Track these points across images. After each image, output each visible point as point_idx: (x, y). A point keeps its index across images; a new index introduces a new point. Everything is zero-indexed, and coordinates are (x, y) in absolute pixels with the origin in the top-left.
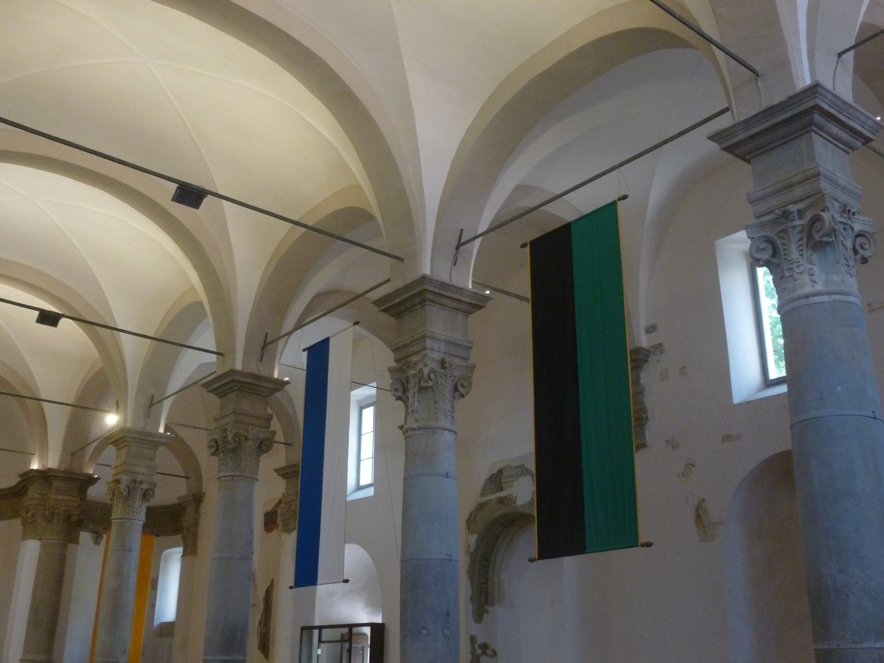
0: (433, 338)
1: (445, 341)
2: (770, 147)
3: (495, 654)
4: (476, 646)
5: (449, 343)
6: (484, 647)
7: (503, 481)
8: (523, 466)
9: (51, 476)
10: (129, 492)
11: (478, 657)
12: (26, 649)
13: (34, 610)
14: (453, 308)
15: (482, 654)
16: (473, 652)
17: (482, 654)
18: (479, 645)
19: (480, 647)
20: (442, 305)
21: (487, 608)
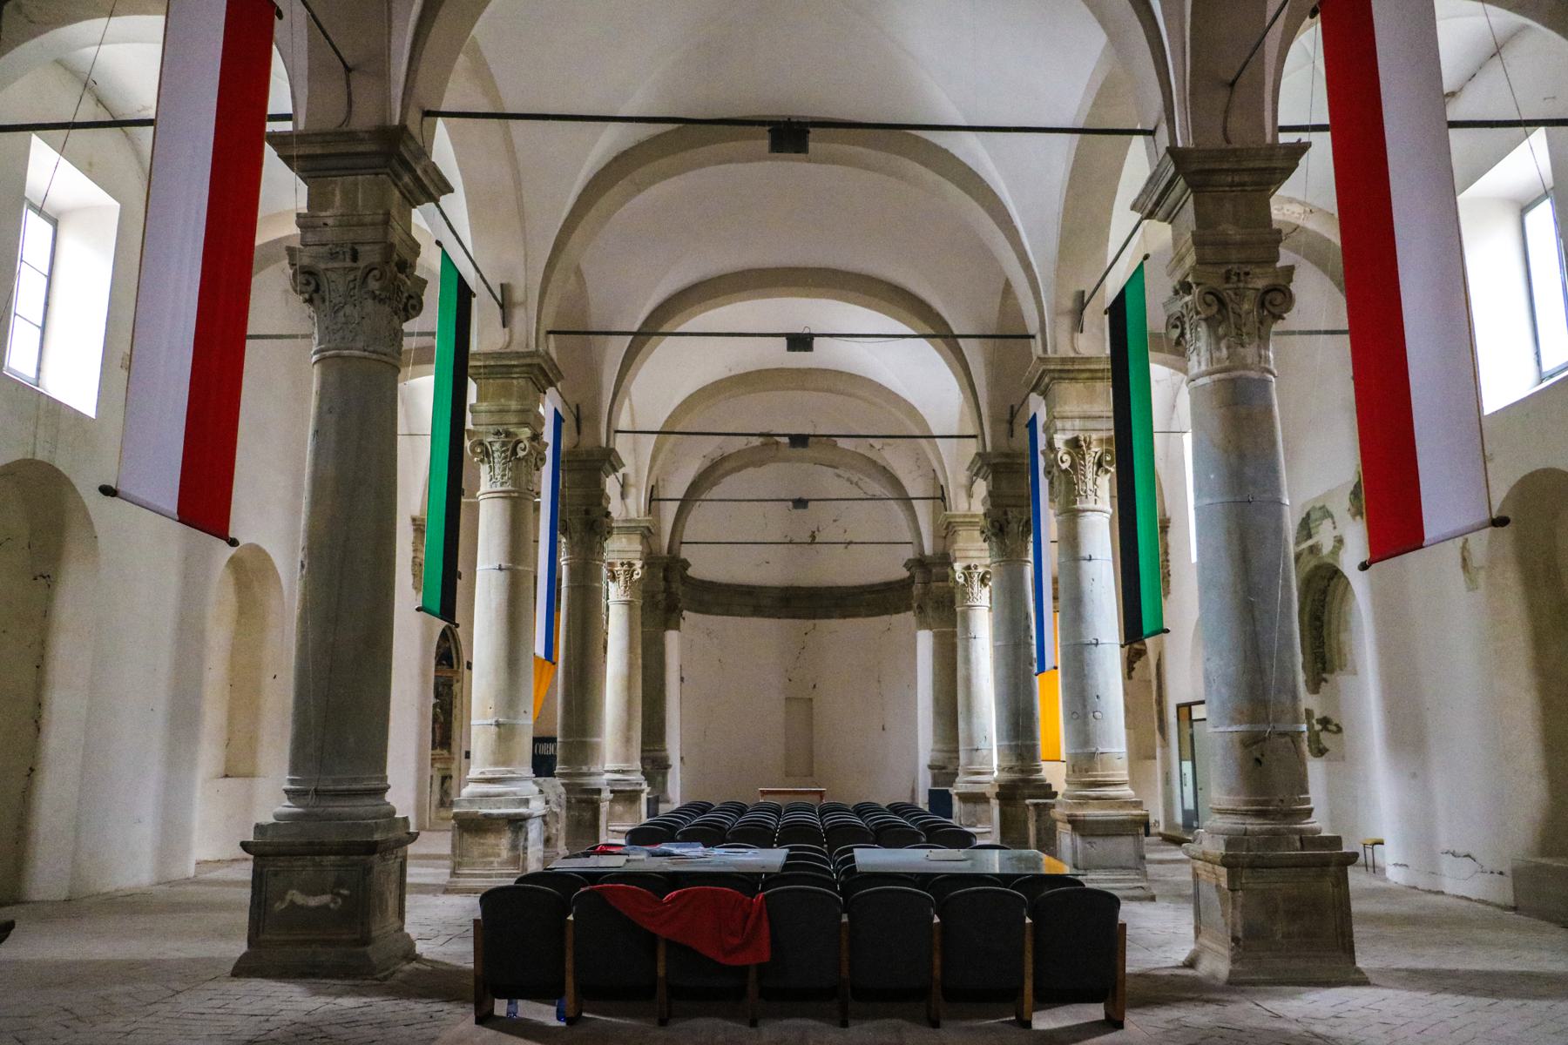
0: (1063, 418)
1: (1080, 418)
2: (1175, 212)
3: (1339, 730)
4: (1314, 721)
5: (1084, 418)
6: (1325, 722)
7: (1312, 525)
8: (1324, 507)
9: (927, 564)
10: (966, 580)
11: (1317, 734)
12: (935, 742)
13: (936, 701)
14: (1088, 379)
15: (1322, 730)
17: (1322, 730)
18: (1317, 720)
19: (1319, 721)
21: (1324, 675)
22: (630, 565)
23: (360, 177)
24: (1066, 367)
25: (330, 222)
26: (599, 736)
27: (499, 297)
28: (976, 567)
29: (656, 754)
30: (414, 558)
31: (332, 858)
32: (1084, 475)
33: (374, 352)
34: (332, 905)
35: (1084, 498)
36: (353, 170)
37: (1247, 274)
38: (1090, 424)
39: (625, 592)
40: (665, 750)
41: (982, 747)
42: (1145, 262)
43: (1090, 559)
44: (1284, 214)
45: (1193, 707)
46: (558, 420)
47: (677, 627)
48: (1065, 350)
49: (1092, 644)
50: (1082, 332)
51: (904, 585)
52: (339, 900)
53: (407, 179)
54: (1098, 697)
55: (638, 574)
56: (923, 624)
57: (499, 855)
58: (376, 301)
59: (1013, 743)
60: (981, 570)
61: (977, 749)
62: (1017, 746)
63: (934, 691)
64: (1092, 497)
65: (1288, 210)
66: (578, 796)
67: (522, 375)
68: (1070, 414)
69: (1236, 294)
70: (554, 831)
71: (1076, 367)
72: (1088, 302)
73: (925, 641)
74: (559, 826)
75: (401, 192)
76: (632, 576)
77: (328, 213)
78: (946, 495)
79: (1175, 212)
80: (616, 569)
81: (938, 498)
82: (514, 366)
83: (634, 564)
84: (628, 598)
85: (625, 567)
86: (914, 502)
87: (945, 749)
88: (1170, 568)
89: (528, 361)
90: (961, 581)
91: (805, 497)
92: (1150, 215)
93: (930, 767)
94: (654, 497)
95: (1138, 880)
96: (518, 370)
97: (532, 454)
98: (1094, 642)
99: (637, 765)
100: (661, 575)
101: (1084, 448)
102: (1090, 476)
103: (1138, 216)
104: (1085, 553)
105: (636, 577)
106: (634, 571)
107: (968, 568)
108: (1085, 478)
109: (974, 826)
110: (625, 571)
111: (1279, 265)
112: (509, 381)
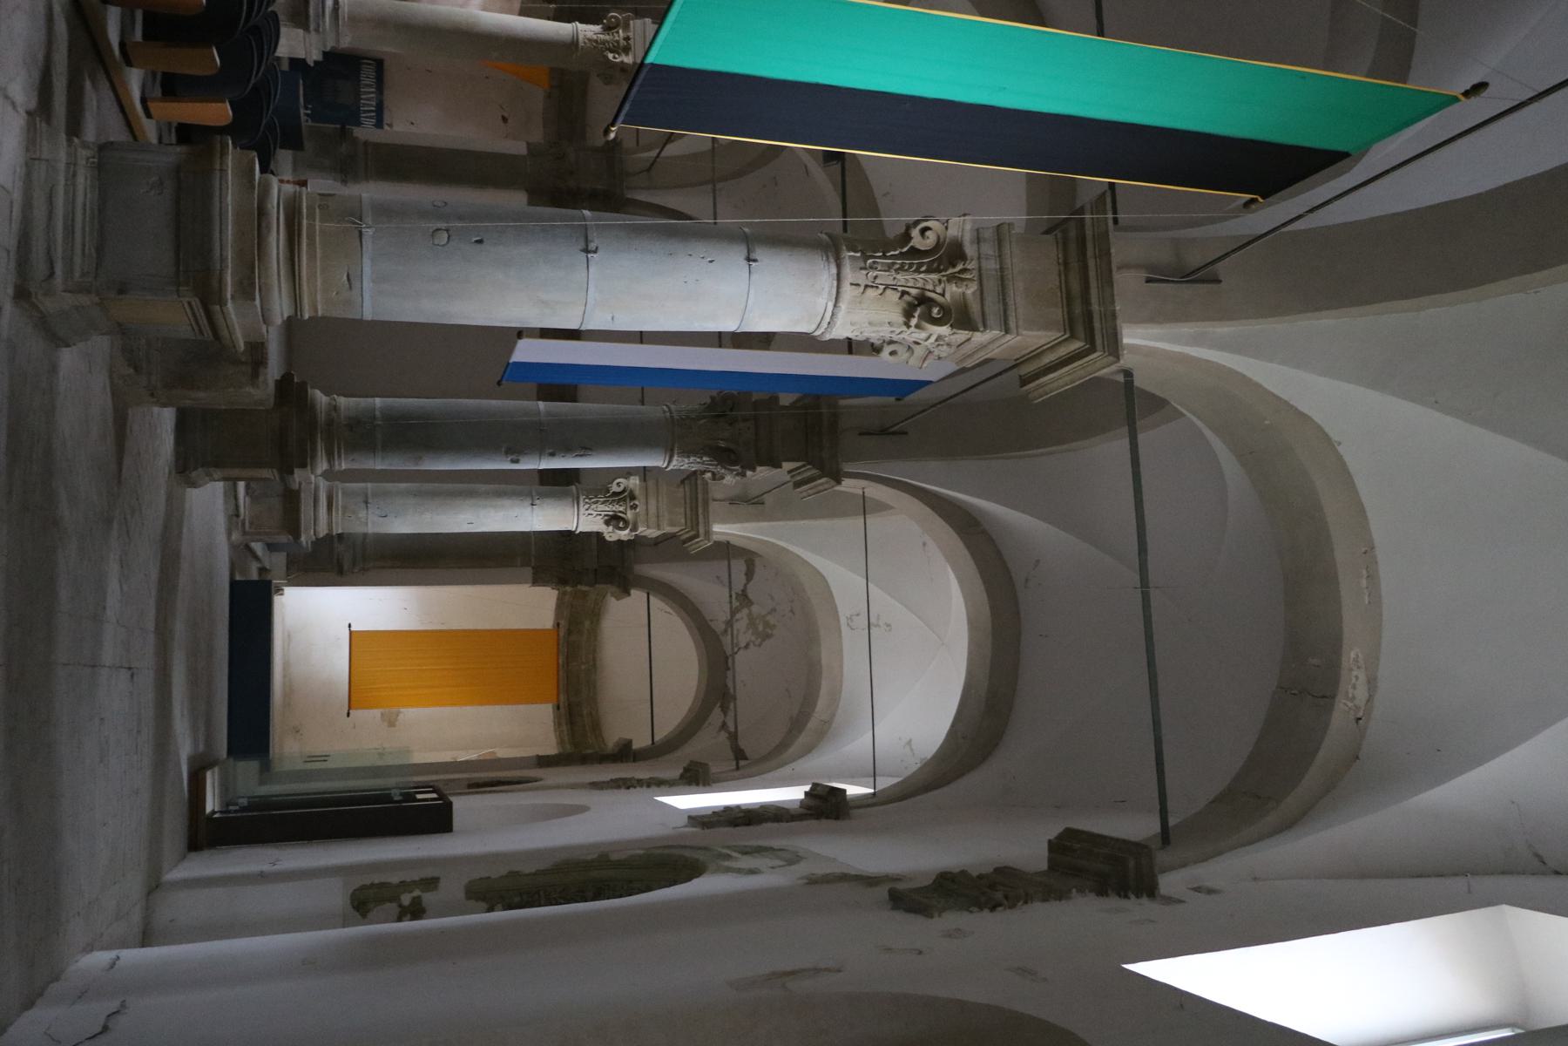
4: (416, 893)
5: (1002, 279)
10: (615, 494)
11: (395, 898)
15: (400, 906)
16: (405, 886)
17: (400, 906)
20: (1066, 264)
22: (626, 50)
24: (1090, 246)
28: (634, 507)
32: (901, 269)
35: (862, 265)
38: (991, 286)
39: (589, 40)
41: (370, 511)
43: (749, 259)
44: (1351, 670)
48: (1123, 248)
49: (587, 241)
50: (1149, 281)
54: (480, 242)
55: (614, 58)
59: (377, 413)
60: (630, 515)
61: (366, 502)
62: (374, 418)
64: (861, 277)
65: (1357, 677)
68: (1007, 251)
71: (1091, 263)
80: (621, 31)
83: (627, 54)
84: (581, 44)
85: (623, 43)
87: (367, 541)
88: (638, 789)
90: (615, 488)
95: (69, 271)
98: (592, 246)
99: (346, 42)
100: (600, 187)
101: (951, 271)
102: (902, 278)
104: (759, 253)
105: (610, 56)
106: (619, 54)
107: (633, 497)
108: (897, 271)
110: (618, 42)
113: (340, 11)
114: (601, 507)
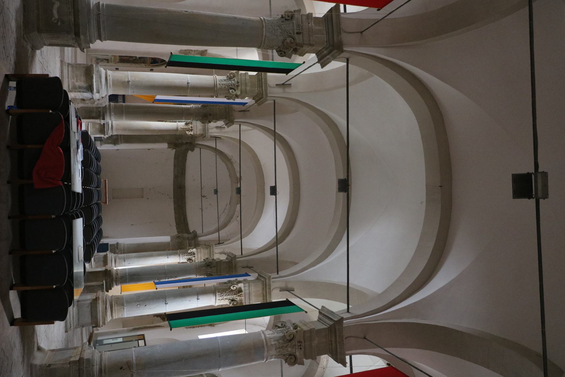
9: (195, 239)
10: (190, 253)
12: (127, 245)
22: (192, 130)
23: (325, 36)
25: (310, 25)
26: (125, 120)
27: (286, 83)
29: (120, 140)
30: (192, 50)
31: (73, 19)
32: (229, 295)
33: (265, 39)
34: (53, 19)
35: (220, 295)
36: (328, 33)
37: (301, 349)
38: (247, 296)
39: (181, 128)
40: (121, 143)
41: (125, 263)
42: (304, 312)
43: (198, 299)
44: (323, 359)
45: (143, 340)
46: (244, 104)
47: (169, 147)
48: (273, 285)
49: (166, 302)
50: (280, 291)
51: (187, 231)
52: (56, 21)
53: (325, 52)
54: (146, 305)
55: (188, 133)
56: (172, 238)
57: (77, 81)
58: (283, 41)
59: (127, 274)
60: (193, 258)
61: (124, 261)
62: (126, 276)
63: (147, 243)
64: (220, 298)
65: (324, 360)
66: (101, 111)
67: (259, 91)
68: (250, 288)
69: (294, 345)
70: (87, 102)
72: (291, 293)
73: (166, 239)
74: (90, 104)
75: (320, 50)
76: (188, 131)
77: (313, 25)
78: (221, 244)
79: (322, 322)
81: (219, 242)
82: (262, 89)
83: (192, 131)
84: (179, 129)
85: (191, 128)
86: (218, 233)
87: (125, 248)
88: (196, 328)
89: (264, 93)
90: (189, 252)
91: (218, 194)
92: (320, 313)
93: (117, 243)
94: (217, 138)
95: (74, 325)
96: (261, 89)
97: (230, 95)
98: (167, 303)
99: (115, 133)
100: (188, 141)
101: (238, 294)
102: (229, 297)
103: (320, 308)
104: (200, 297)
105: (187, 132)
106: (189, 131)
107: (194, 254)
108: (228, 295)
109: (94, 261)
110: (189, 128)
111: (304, 360)
112: (257, 87)
113: (113, 128)
114: (186, 257)
